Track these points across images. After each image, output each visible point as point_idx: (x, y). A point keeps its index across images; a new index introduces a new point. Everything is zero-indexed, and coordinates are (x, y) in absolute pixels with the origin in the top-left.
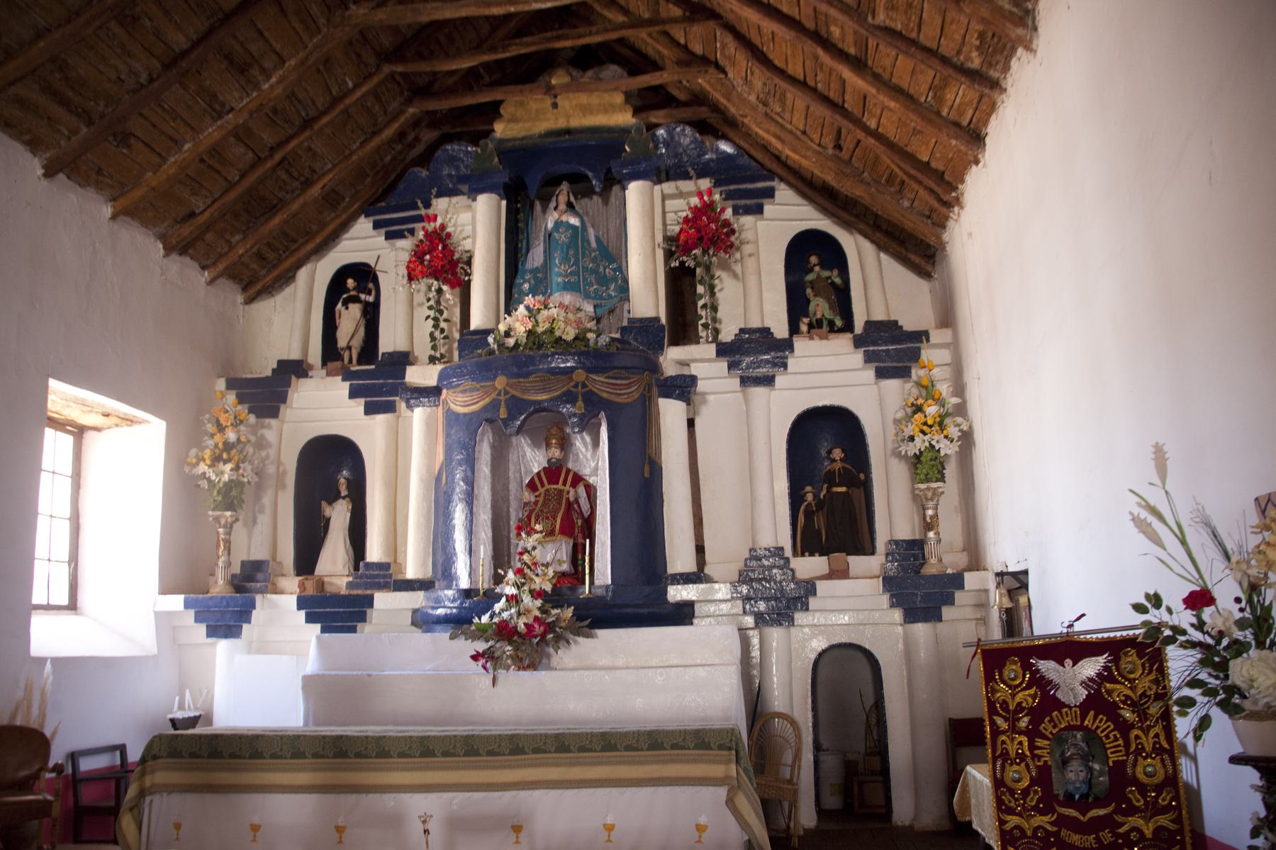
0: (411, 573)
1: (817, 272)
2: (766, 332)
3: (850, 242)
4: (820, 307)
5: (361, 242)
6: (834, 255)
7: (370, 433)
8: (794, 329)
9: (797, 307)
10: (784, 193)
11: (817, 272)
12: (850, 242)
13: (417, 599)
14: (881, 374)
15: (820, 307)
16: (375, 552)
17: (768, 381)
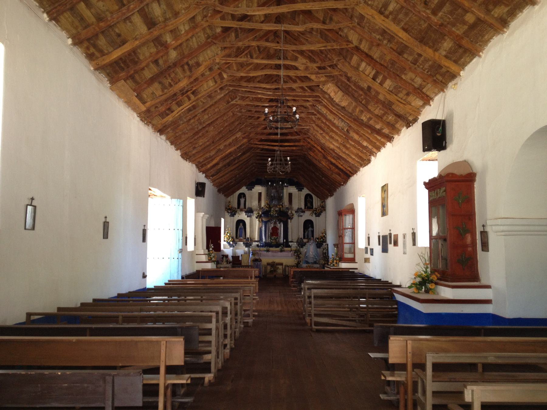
0: (256, 239)
1: (309, 199)
2: (301, 209)
3: (314, 196)
4: (309, 205)
5: (244, 190)
6: (311, 197)
7: (247, 221)
8: (305, 208)
9: (306, 205)
10: (305, 188)
11: (309, 199)
12: (314, 196)
13: (257, 243)
14: (316, 216)
15: (309, 205)
16: (248, 235)
17: (301, 216)
